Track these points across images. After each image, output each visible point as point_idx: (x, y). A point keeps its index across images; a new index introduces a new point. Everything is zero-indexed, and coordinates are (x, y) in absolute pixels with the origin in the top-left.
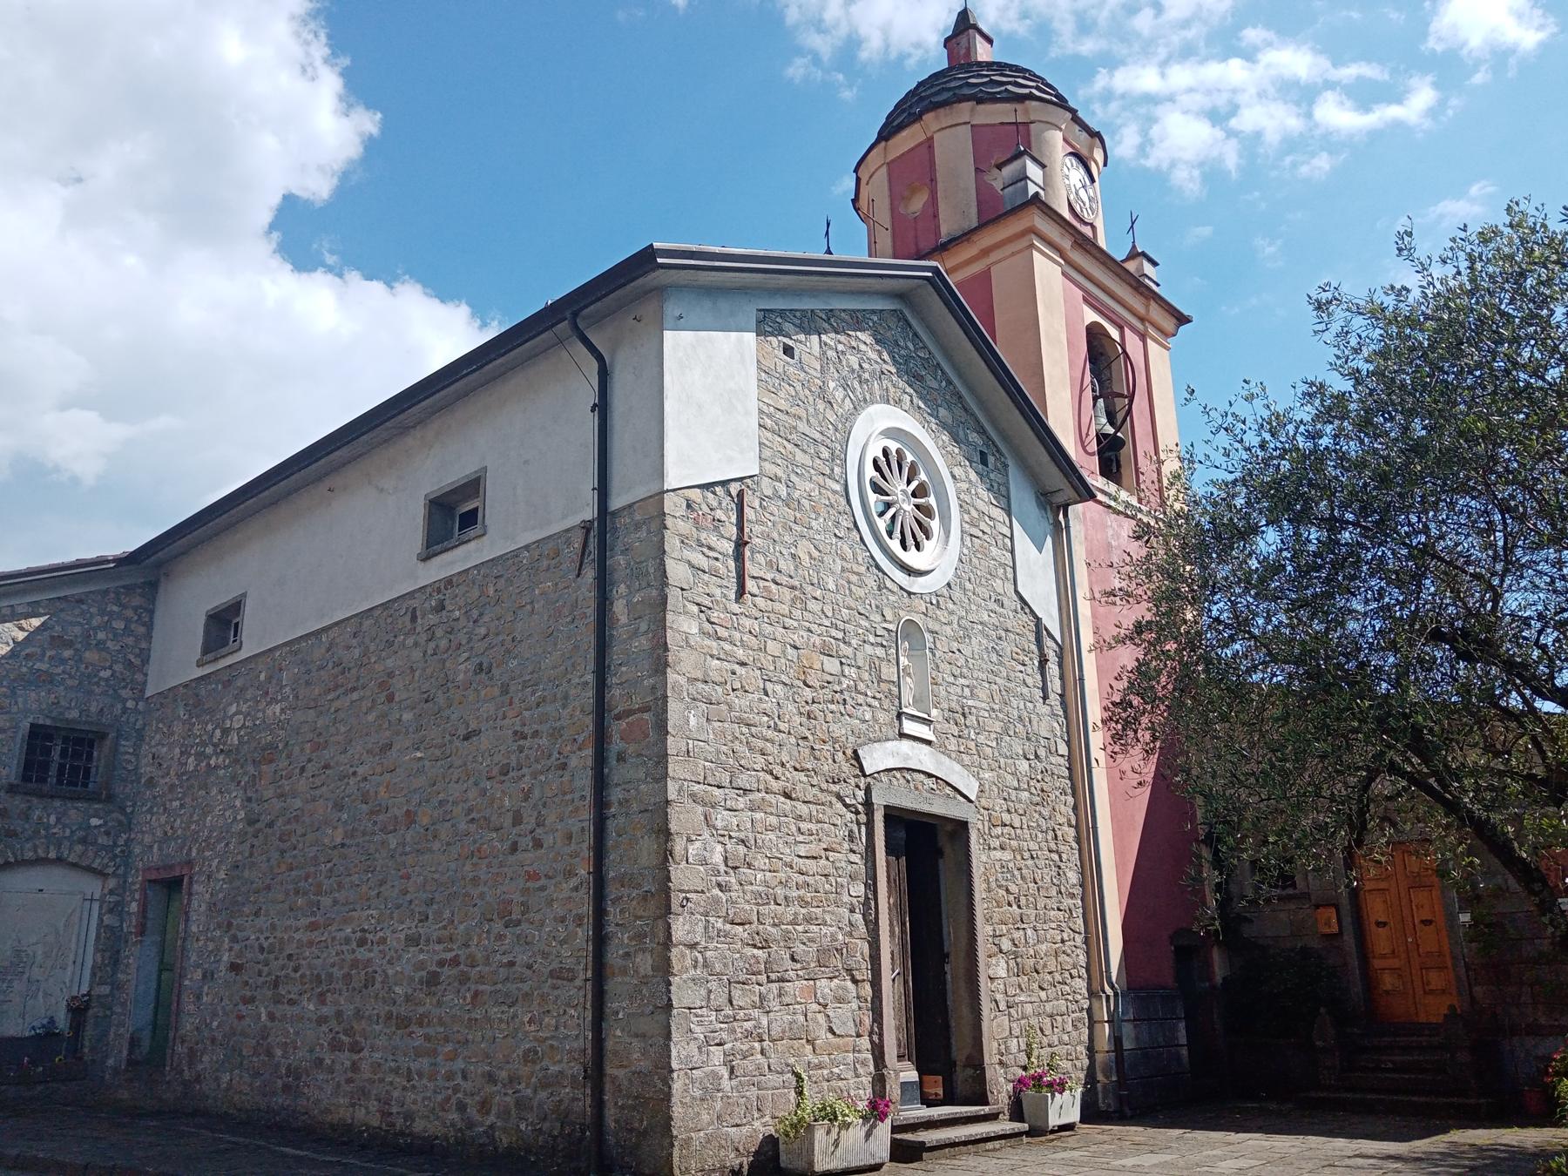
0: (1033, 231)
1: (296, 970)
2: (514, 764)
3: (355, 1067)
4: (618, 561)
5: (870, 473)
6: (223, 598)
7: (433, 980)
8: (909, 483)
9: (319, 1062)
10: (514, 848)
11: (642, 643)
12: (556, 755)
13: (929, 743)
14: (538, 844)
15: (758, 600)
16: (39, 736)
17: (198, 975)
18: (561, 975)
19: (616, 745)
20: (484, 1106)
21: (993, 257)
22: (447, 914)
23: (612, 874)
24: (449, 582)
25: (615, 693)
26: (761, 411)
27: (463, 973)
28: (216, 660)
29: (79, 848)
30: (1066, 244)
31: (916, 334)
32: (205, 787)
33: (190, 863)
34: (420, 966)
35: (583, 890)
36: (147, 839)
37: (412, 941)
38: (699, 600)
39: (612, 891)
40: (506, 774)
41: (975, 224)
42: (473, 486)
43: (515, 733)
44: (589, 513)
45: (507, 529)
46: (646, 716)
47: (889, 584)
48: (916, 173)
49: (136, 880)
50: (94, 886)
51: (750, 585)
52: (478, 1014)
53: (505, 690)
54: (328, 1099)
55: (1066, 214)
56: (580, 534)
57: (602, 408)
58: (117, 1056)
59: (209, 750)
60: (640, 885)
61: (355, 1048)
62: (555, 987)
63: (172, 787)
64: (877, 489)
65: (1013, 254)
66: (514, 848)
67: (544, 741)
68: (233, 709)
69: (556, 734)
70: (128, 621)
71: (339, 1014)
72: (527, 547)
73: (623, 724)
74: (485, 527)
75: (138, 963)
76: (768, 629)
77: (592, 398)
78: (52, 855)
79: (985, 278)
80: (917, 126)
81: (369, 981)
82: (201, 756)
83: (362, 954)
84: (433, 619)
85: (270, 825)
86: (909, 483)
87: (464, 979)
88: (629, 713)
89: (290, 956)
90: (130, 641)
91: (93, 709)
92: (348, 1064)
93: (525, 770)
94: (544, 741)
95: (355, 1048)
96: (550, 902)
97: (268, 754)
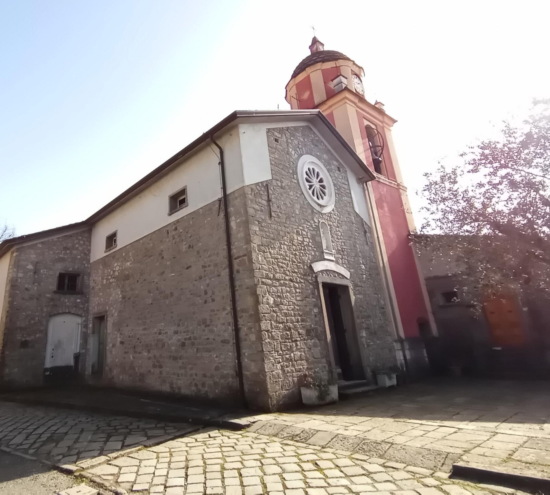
0: (346, 98)
1: (140, 343)
2: (203, 275)
3: (161, 373)
4: (231, 209)
5: (305, 176)
6: (110, 232)
7: (183, 344)
8: (317, 178)
9: (150, 371)
10: (206, 302)
11: (241, 235)
12: (216, 272)
13: (332, 261)
14: (213, 300)
15: (276, 219)
16: (62, 277)
17: (111, 345)
18: (224, 342)
19: (236, 267)
20: (203, 385)
21: (333, 108)
22: (186, 324)
23: (239, 309)
24: (178, 221)
25: (234, 251)
26: (270, 160)
27: (192, 342)
28: (110, 250)
29: (74, 309)
30: (356, 101)
31: (314, 132)
32: (109, 288)
33: (106, 312)
34: (179, 340)
35: (229, 314)
36: (93, 305)
37: (176, 332)
38: (258, 220)
39: (239, 314)
40: (201, 279)
41: (326, 99)
42: (183, 192)
43: (203, 266)
44: (220, 195)
45: (195, 203)
46: (245, 258)
47: (315, 211)
48: (306, 85)
49: (91, 317)
50: (79, 320)
51: (273, 214)
52: (199, 355)
53: (198, 252)
54: (154, 383)
55: (355, 91)
56: (218, 202)
57: (222, 163)
58: (89, 371)
59: (110, 277)
60: (248, 312)
61: (161, 367)
62: (223, 346)
63: (99, 289)
64: (308, 181)
65: (340, 106)
66: (206, 302)
67: (212, 268)
68: (116, 265)
69: (216, 265)
70: (84, 241)
71: (155, 356)
72: (201, 208)
73: (238, 260)
74: (188, 203)
75: (92, 342)
76: (280, 228)
77: (218, 160)
78: (67, 311)
79: (331, 115)
80: (304, 72)
81: (163, 345)
82: (107, 279)
83: (160, 337)
84: (174, 233)
85: (129, 299)
86: (317, 178)
87: (193, 344)
88: (239, 257)
89: (138, 339)
90: (85, 247)
91: (76, 267)
92: (158, 372)
93: (207, 277)
94: (212, 268)
95: (161, 367)
96: (219, 319)
97: (127, 277)
